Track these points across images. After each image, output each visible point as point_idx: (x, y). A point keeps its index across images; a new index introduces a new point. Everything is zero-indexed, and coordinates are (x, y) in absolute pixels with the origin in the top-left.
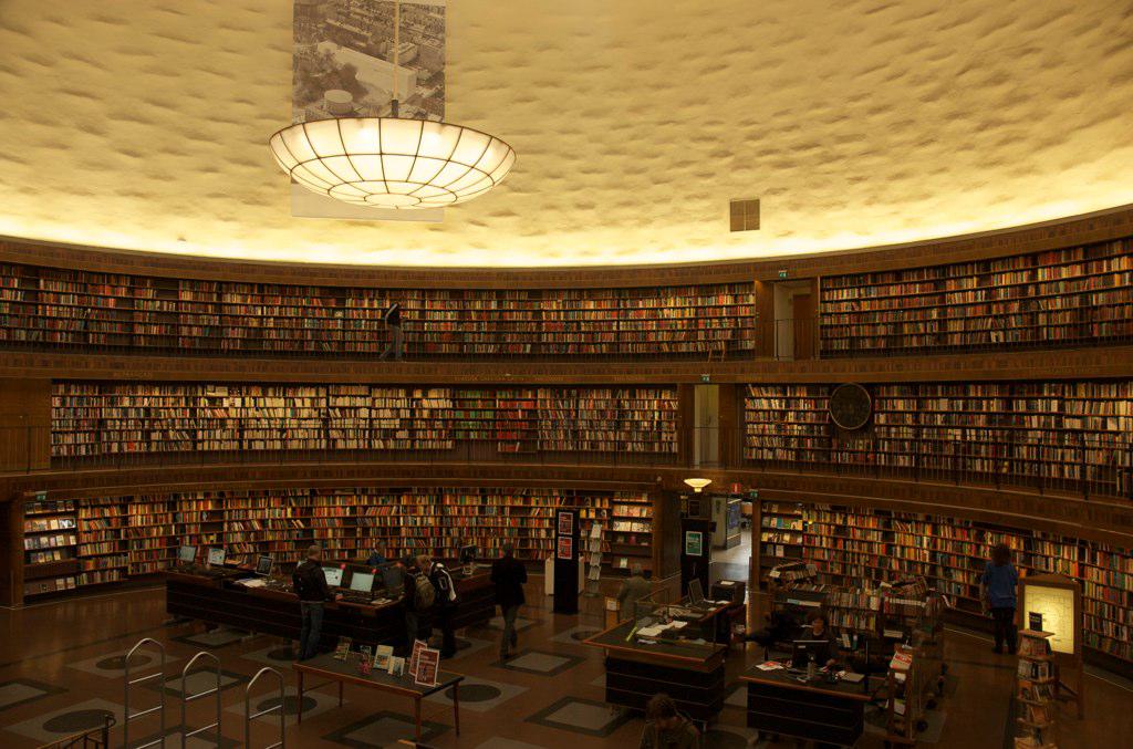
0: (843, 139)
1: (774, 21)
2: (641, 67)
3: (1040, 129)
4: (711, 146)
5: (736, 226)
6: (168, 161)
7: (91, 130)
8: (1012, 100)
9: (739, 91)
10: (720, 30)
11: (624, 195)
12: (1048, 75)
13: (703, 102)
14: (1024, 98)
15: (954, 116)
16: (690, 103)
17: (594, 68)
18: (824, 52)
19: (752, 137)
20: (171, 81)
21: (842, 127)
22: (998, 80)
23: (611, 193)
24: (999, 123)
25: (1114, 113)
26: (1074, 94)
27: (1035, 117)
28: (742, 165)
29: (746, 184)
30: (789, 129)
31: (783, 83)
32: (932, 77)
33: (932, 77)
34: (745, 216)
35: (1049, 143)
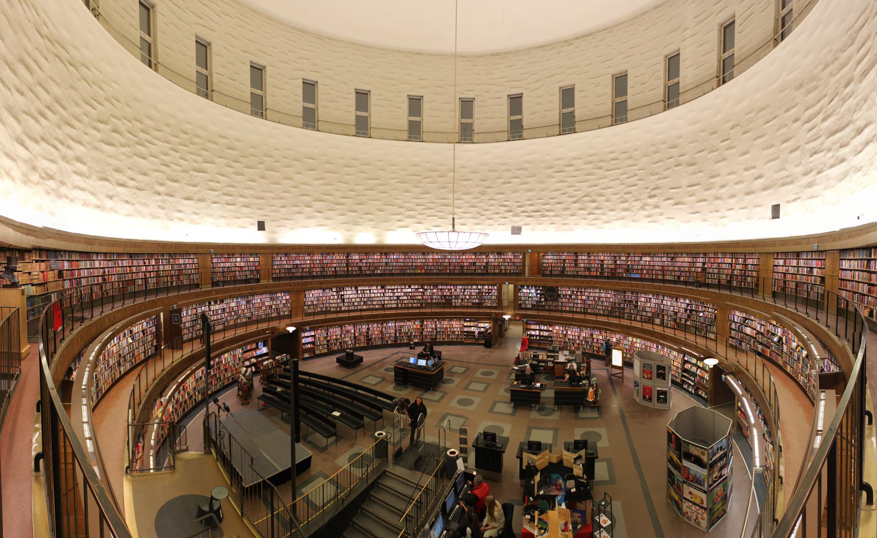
0: (548, 211)
1: (526, 170)
2: (482, 180)
3: (604, 217)
4: (506, 208)
5: (513, 233)
6: (330, 213)
7: (308, 206)
8: (597, 208)
9: (515, 191)
10: (509, 170)
11: (477, 221)
12: (606, 203)
13: (503, 194)
14: (600, 208)
15: (581, 209)
16: (499, 194)
17: (467, 180)
18: (542, 182)
19: (519, 207)
20: (330, 187)
21: (547, 207)
22: (594, 201)
23: (473, 220)
24: (594, 214)
25: (623, 219)
26: (613, 210)
27: (604, 214)
28: (516, 215)
29: (518, 221)
30: (531, 205)
31: (529, 190)
32: (575, 196)
33: (575, 196)
34: (516, 230)
35: (607, 222)
